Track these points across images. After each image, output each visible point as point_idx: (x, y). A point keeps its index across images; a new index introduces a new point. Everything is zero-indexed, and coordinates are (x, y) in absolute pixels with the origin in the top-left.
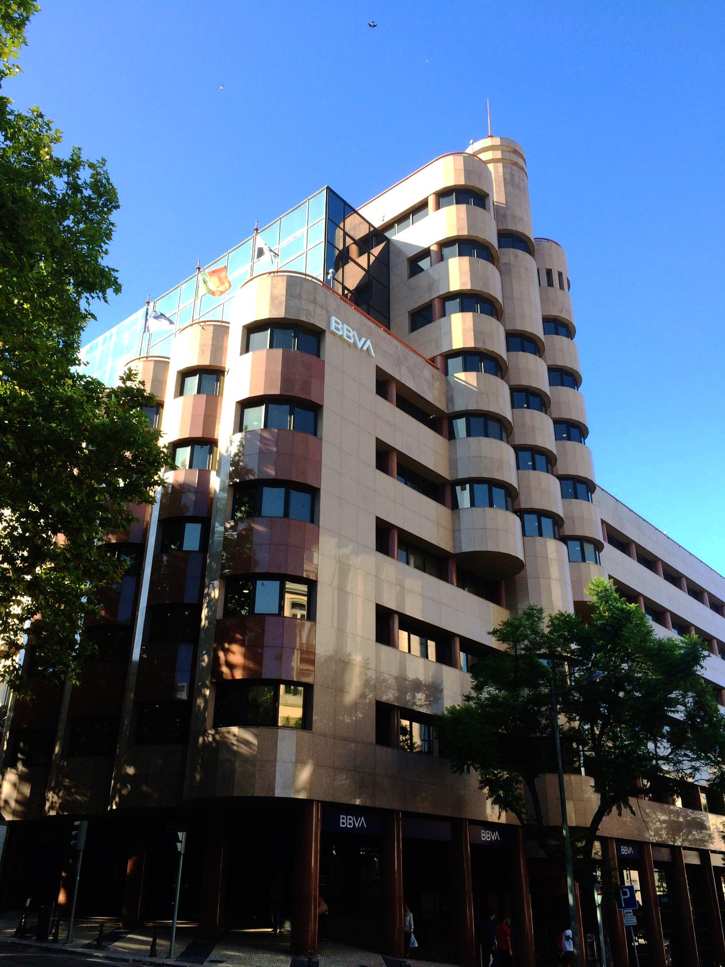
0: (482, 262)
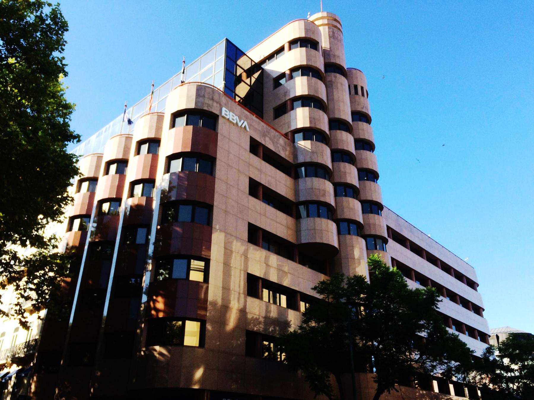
0: (314, 80)
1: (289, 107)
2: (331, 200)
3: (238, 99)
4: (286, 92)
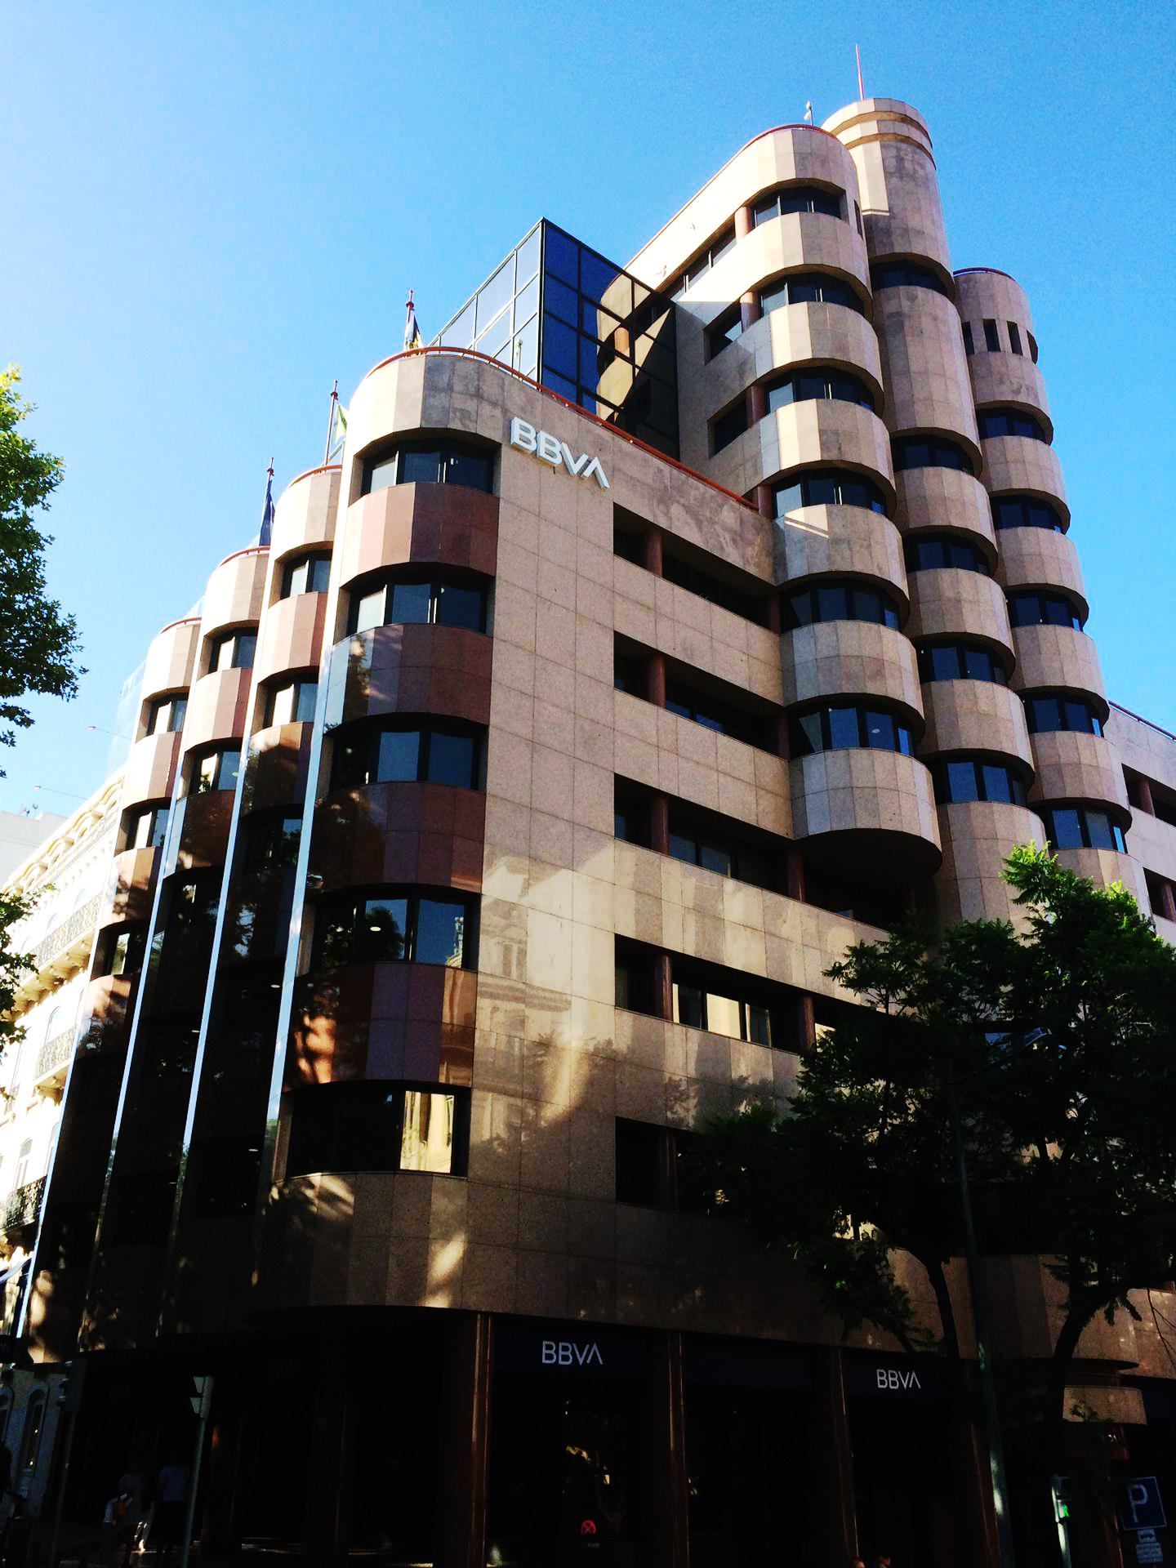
0: (833, 311)
1: (754, 408)
2: (908, 692)
3: (604, 412)
4: (744, 363)
